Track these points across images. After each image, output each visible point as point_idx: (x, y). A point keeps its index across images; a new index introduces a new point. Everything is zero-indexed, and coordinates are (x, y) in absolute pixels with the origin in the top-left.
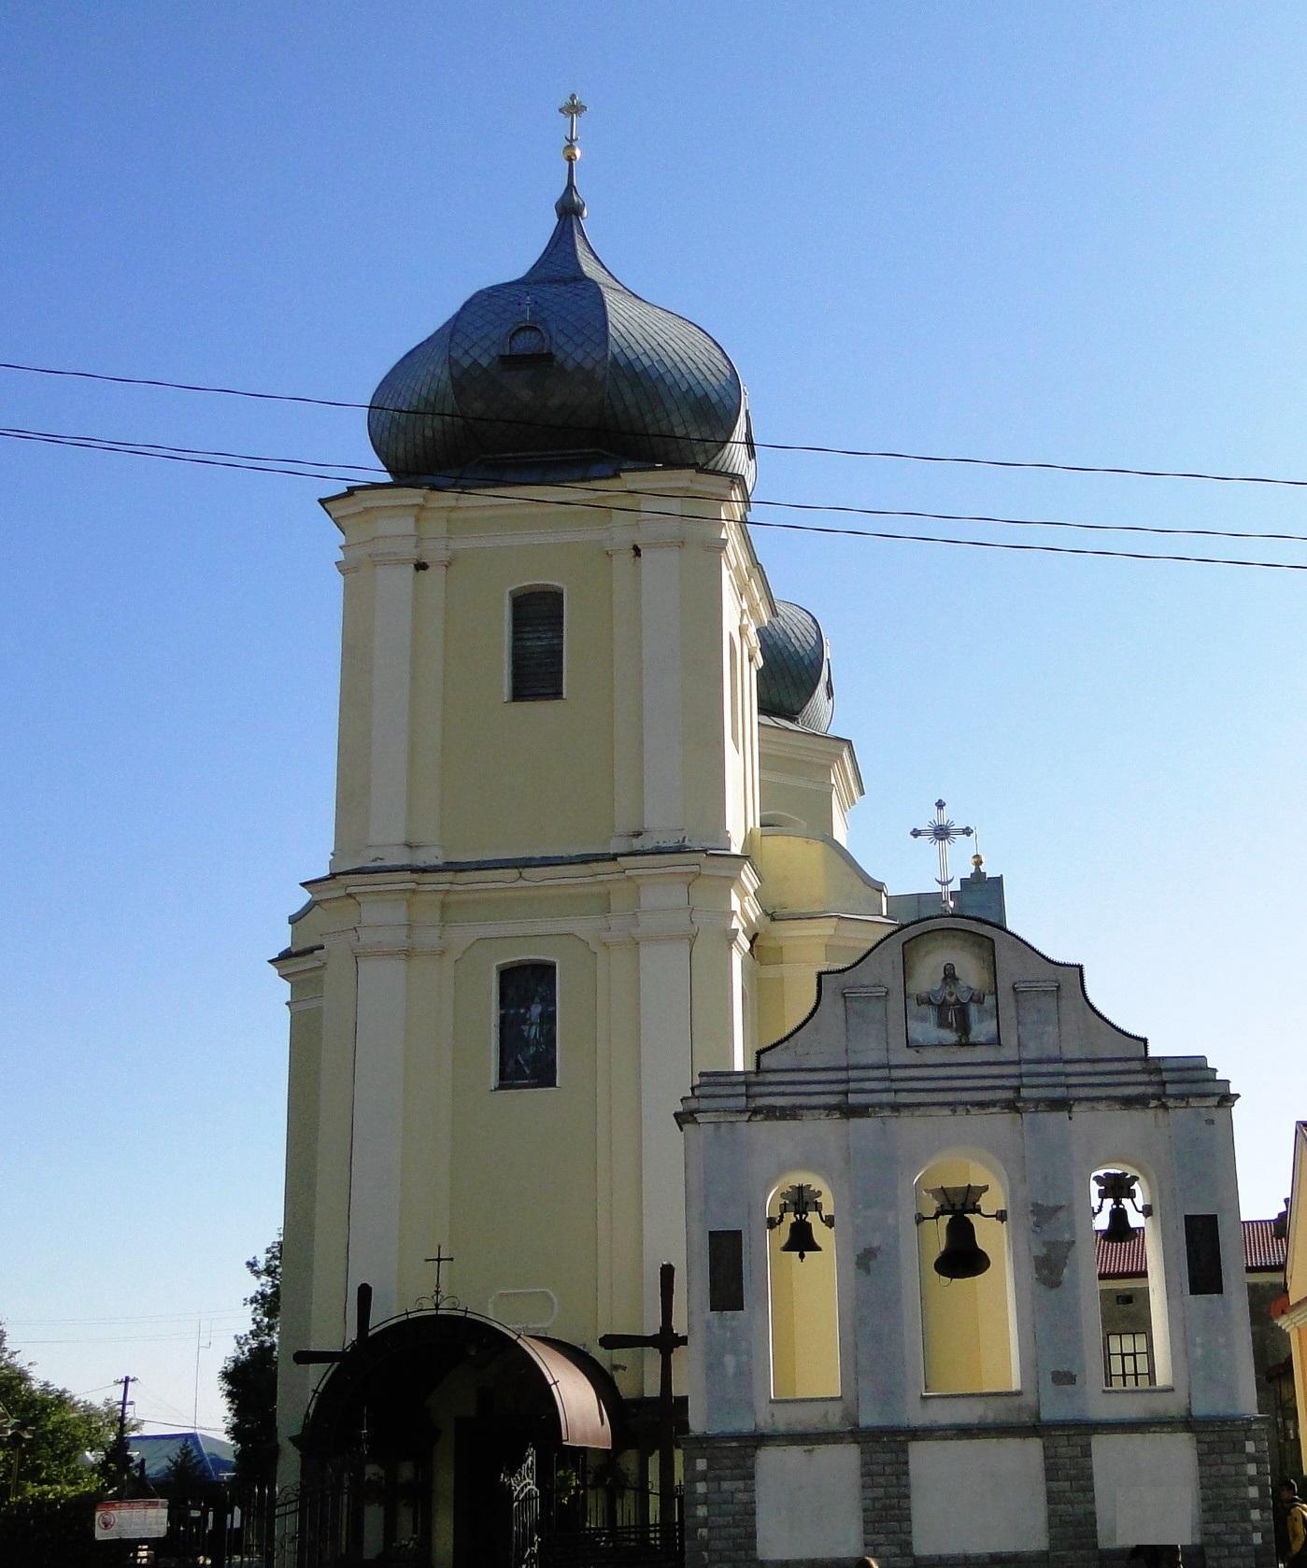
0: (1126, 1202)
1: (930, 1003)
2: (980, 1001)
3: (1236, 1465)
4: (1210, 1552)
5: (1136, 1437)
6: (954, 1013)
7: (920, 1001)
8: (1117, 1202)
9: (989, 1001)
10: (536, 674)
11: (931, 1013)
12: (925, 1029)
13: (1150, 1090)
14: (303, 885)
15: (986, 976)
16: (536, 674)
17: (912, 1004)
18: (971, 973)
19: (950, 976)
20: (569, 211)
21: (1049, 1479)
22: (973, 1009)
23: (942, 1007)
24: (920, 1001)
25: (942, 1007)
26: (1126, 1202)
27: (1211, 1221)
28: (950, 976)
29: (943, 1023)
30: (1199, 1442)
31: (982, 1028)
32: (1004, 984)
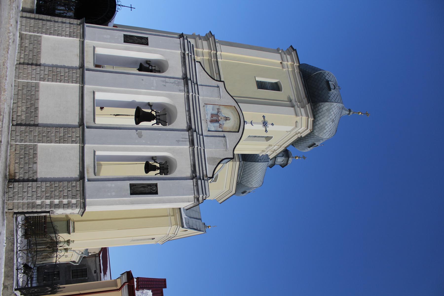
0: (158, 171)
1: (218, 112)
3: (67, 196)
5: (78, 161)
6: (215, 119)
7: (218, 109)
8: (158, 168)
11: (215, 112)
12: (210, 110)
13: (198, 174)
14: (210, 31)
15: (228, 130)
17: (218, 107)
18: (229, 125)
19: (227, 119)
22: (217, 124)
23: (217, 115)
24: (218, 109)
25: (217, 115)
26: (158, 171)
28: (227, 119)
29: (212, 115)
31: (213, 127)
32: (226, 134)
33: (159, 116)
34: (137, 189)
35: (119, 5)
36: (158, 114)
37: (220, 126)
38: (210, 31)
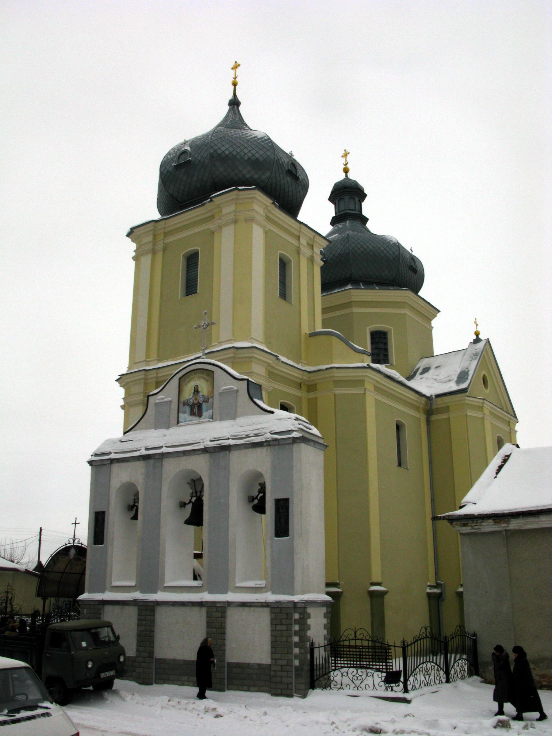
2: (207, 402)
4: (273, 668)
9: (211, 400)
10: (191, 287)
11: (188, 409)
14: (116, 381)
16: (191, 287)
19: (196, 391)
20: (235, 103)
21: (208, 627)
22: (204, 406)
23: (192, 407)
24: (185, 404)
27: (287, 500)
28: (196, 391)
30: (272, 613)
33: (196, 492)
34: (282, 527)
35: (74, 541)
36: (194, 495)
37: (206, 400)
38: (116, 381)
